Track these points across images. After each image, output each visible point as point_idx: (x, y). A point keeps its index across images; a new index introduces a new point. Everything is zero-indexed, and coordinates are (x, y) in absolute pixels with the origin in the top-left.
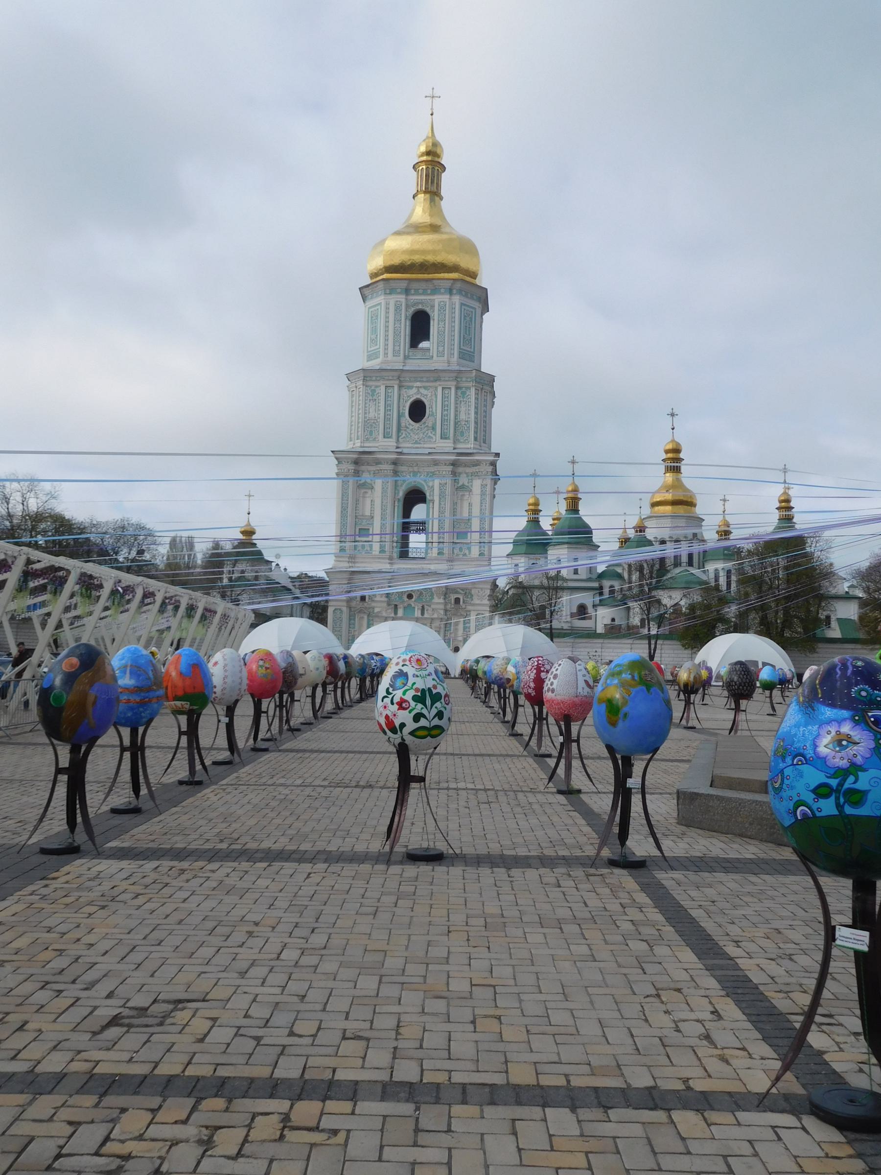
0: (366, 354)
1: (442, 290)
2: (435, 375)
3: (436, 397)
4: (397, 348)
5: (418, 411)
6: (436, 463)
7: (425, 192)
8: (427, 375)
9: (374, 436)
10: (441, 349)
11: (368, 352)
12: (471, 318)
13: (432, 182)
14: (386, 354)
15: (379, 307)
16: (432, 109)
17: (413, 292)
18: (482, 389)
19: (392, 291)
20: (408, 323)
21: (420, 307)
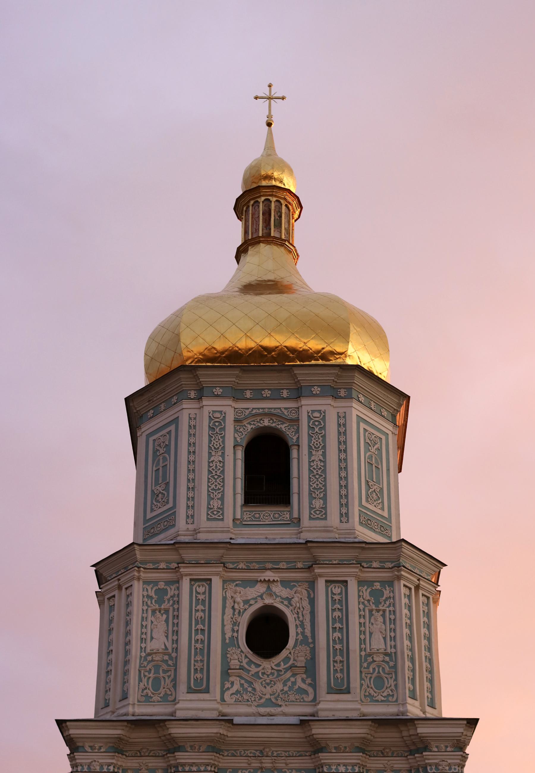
0: (141, 526)
1: (316, 390)
2: (309, 556)
3: (312, 602)
4: (216, 504)
5: (267, 633)
6: (317, 747)
7: (268, 239)
8: (290, 554)
9: (162, 691)
10: (318, 504)
11: (146, 521)
12: (379, 450)
13: (278, 225)
14: (190, 518)
15: (172, 428)
16: (269, 116)
17: (248, 394)
18: (417, 587)
20: (240, 454)
21: (266, 422)
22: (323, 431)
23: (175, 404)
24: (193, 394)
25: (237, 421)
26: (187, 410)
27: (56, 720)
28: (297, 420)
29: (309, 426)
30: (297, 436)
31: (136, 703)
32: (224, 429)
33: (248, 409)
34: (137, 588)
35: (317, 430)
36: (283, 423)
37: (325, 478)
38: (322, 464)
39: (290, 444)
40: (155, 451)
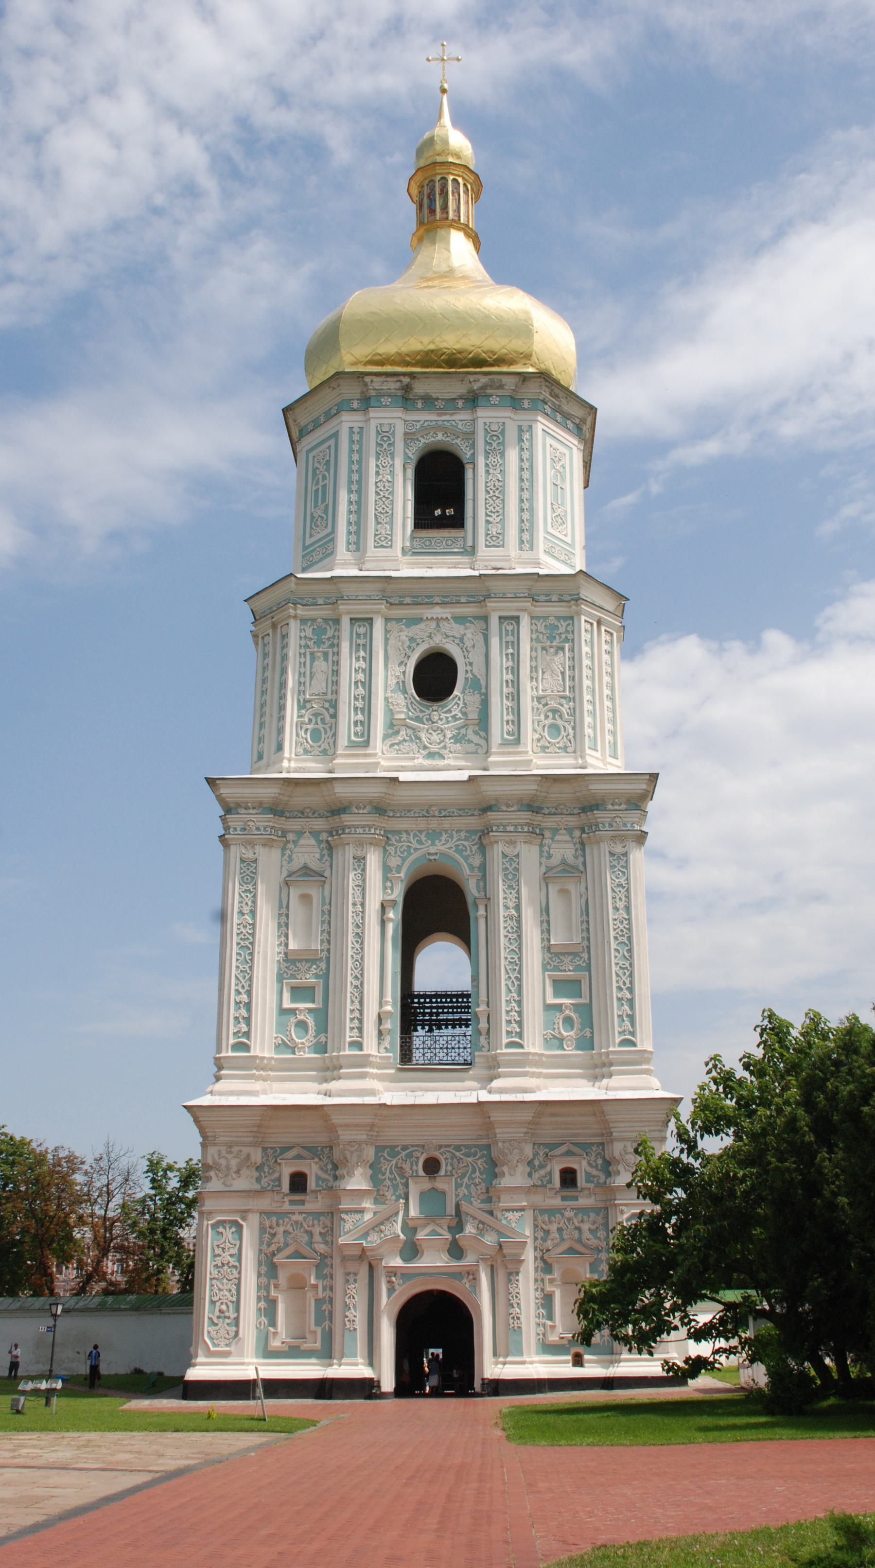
10: (494, 531)
19: (366, 403)
20: (410, 473)
21: (440, 437)
22: (501, 447)
23: (335, 415)
24: (355, 405)
25: (406, 434)
26: (348, 421)
27: (206, 779)
28: (473, 433)
29: (486, 441)
30: (472, 451)
31: (293, 756)
32: (392, 445)
33: (419, 421)
34: (294, 628)
35: (495, 445)
36: (458, 437)
37: (503, 500)
38: (500, 484)
39: (465, 461)
40: (315, 470)
